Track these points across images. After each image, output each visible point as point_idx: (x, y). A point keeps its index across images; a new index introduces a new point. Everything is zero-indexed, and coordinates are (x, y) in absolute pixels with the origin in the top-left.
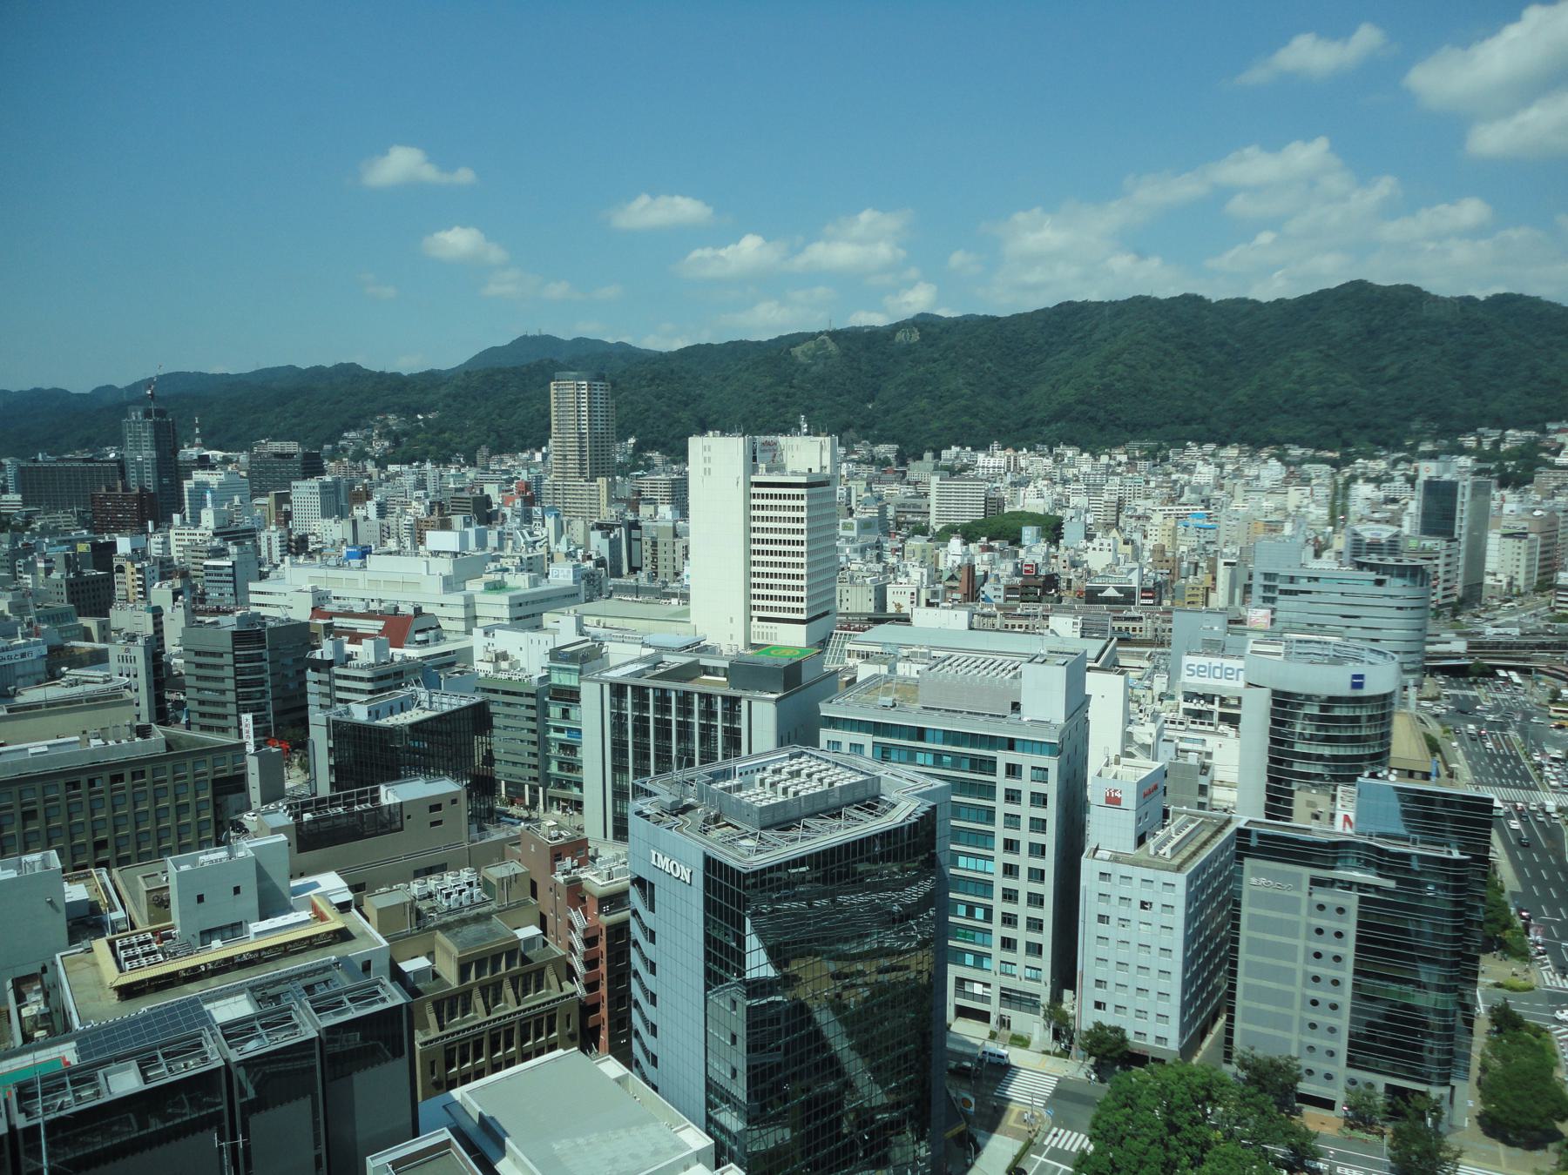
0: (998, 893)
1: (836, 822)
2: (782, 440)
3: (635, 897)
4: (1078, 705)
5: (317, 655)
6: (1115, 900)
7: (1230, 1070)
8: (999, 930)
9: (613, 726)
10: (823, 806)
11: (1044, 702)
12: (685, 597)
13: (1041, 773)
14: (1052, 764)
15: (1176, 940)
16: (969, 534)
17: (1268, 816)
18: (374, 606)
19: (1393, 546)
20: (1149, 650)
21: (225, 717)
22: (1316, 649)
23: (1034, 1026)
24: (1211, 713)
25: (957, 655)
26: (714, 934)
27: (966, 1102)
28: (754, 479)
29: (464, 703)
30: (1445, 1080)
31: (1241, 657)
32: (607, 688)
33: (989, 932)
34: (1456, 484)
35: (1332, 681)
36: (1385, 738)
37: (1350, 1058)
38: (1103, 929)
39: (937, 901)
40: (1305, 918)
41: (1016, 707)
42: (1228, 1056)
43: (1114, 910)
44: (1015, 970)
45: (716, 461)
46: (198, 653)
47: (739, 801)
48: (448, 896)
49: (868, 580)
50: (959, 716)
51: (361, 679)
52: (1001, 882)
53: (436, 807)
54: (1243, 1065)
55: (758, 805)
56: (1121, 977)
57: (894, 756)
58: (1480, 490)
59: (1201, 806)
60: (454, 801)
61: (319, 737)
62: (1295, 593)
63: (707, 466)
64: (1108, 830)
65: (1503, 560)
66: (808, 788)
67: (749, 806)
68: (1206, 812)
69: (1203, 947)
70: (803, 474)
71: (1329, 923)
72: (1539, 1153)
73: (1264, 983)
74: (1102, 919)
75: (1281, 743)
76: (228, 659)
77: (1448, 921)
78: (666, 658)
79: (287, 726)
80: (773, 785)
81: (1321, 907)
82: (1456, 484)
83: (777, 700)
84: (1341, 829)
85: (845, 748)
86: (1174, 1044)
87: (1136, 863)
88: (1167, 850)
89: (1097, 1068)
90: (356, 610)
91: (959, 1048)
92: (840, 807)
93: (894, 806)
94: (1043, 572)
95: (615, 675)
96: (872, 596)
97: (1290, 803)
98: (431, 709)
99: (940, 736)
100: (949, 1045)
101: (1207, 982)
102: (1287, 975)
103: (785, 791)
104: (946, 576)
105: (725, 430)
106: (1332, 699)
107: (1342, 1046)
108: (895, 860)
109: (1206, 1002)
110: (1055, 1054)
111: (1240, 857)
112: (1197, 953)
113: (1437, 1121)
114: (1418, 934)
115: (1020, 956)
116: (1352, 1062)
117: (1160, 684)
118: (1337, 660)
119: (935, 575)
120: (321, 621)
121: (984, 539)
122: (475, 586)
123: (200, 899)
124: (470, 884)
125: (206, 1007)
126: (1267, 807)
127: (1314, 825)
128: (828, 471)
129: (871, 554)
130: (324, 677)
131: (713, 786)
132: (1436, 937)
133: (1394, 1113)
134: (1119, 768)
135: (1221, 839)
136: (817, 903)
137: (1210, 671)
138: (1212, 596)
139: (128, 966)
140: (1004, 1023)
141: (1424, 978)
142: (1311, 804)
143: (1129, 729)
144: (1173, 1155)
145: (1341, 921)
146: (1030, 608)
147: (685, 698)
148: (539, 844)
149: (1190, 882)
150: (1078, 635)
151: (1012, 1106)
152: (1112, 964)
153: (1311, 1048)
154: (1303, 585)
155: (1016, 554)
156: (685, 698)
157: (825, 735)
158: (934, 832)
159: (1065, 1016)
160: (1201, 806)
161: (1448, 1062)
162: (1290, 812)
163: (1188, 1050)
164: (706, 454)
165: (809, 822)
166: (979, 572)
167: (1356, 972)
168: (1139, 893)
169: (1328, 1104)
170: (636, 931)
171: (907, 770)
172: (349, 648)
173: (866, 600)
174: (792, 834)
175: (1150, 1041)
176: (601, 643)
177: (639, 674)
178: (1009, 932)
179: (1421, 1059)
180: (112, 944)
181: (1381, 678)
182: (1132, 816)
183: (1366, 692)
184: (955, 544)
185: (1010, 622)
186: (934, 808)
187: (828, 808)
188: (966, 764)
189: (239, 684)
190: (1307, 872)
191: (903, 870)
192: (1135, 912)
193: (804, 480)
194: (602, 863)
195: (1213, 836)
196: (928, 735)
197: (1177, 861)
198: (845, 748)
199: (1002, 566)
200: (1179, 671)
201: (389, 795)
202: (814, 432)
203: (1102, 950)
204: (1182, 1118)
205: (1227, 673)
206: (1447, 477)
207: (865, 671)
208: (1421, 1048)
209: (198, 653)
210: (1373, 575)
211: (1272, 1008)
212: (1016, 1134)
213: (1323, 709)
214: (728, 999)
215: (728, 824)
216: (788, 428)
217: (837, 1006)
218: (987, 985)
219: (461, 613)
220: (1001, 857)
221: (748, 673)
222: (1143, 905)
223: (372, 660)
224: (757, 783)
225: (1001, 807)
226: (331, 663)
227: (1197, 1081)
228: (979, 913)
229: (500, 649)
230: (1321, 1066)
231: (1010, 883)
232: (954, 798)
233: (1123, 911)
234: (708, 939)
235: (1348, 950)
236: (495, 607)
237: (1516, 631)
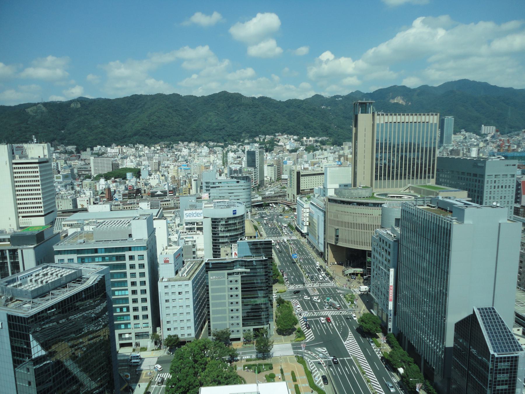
0: (130, 301)
1: (65, 289)
2: (25, 146)
4: (152, 232)
6: (170, 294)
7: (211, 338)
8: (132, 313)
10: (59, 285)
11: (140, 232)
13: (141, 257)
14: (145, 253)
15: (191, 302)
16: (107, 177)
17: (214, 257)
19: (240, 171)
20: (173, 211)
22: (222, 204)
23: (148, 343)
24: (194, 228)
25: (107, 220)
27: (127, 376)
28: (14, 161)
30: (267, 323)
31: (201, 209)
33: (129, 315)
35: (227, 213)
36: (243, 228)
37: (243, 324)
38: (167, 304)
39: (109, 309)
40: (227, 286)
41: (130, 236)
42: (210, 333)
43: (170, 297)
44: (139, 326)
47: (21, 290)
50: (110, 242)
52: (131, 297)
54: (214, 335)
55: (30, 290)
56: (175, 318)
57: (86, 260)
58: (261, 153)
59: (194, 258)
62: (215, 187)
64: (166, 271)
65: (269, 173)
66: (51, 279)
67: (26, 291)
68: (196, 260)
69: (199, 302)
70: (36, 159)
71: (233, 286)
72: (291, 336)
73: (218, 308)
74: (167, 301)
75: (215, 234)
77: (263, 278)
80: (36, 281)
81: (231, 281)
83: (34, 248)
84: (234, 257)
85: (66, 261)
86: (193, 335)
87: (176, 280)
88: (185, 274)
89: (170, 350)
91: (122, 358)
92: (66, 284)
93: (88, 279)
94: (135, 188)
96: (71, 203)
97: (219, 252)
99: (103, 250)
100: (119, 358)
101: (201, 313)
102: (223, 304)
103: (42, 282)
104: (100, 192)
106: (228, 219)
107: (240, 321)
108: (91, 298)
109: (201, 319)
110: (156, 350)
111: (207, 271)
112: (197, 304)
113: (266, 336)
114: (257, 283)
115: (141, 321)
116: (244, 325)
117: (178, 221)
118: (228, 207)
119: (96, 193)
121: (113, 178)
126: (213, 254)
127: (227, 257)
128: (47, 157)
129: (68, 187)
131: (9, 286)
132: (262, 283)
133: (256, 336)
134: (167, 250)
135: (201, 267)
136: (61, 322)
137: (193, 215)
138: (191, 190)
140: (137, 344)
141: (260, 295)
142: (225, 251)
143: (169, 237)
144: (196, 370)
146: (132, 201)
149: (193, 282)
150: (150, 208)
151: (143, 372)
152: (171, 315)
153: (232, 324)
154: (217, 185)
155: (125, 183)
157: (57, 258)
158: (105, 285)
159: (158, 336)
160: (194, 258)
161: (268, 317)
162: (220, 255)
163: (197, 336)
165: (53, 292)
166: (112, 190)
167: (242, 298)
168: (177, 290)
169: (239, 339)
171: (92, 265)
174: (47, 298)
175: (186, 336)
178: (136, 313)
179: (261, 319)
181: (241, 210)
182: (173, 265)
183: (237, 215)
184: (102, 181)
185: (125, 207)
186: (104, 276)
187: (61, 285)
188: (114, 258)
191: (94, 301)
192: (177, 296)
193: (37, 161)
195: (198, 267)
196: (99, 251)
197: (189, 277)
198: (66, 261)
199: (121, 187)
202: (39, 141)
203: (168, 311)
204: (198, 357)
205: (198, 215)
206: (252, 150)
207: (71, 231)
208: (261, 316)
210: (236, 180)
212: (145, 381)
213: (226, 222)
214: (25, 369)
216: (28, 140)
217: (74, 358)
218: (130, 334)
220: (130, 288)
221: (19, 239)
222: (179, 293)
224: (29, 281)
225: (128, 271)
227: (201, 344)
228: (125, 310)
230: (235, 329)
231: (135, 297)
232: (111, 271)
233: (173, 297)
234: (13, 348)
235: (239, 292)
237: (273, 193)
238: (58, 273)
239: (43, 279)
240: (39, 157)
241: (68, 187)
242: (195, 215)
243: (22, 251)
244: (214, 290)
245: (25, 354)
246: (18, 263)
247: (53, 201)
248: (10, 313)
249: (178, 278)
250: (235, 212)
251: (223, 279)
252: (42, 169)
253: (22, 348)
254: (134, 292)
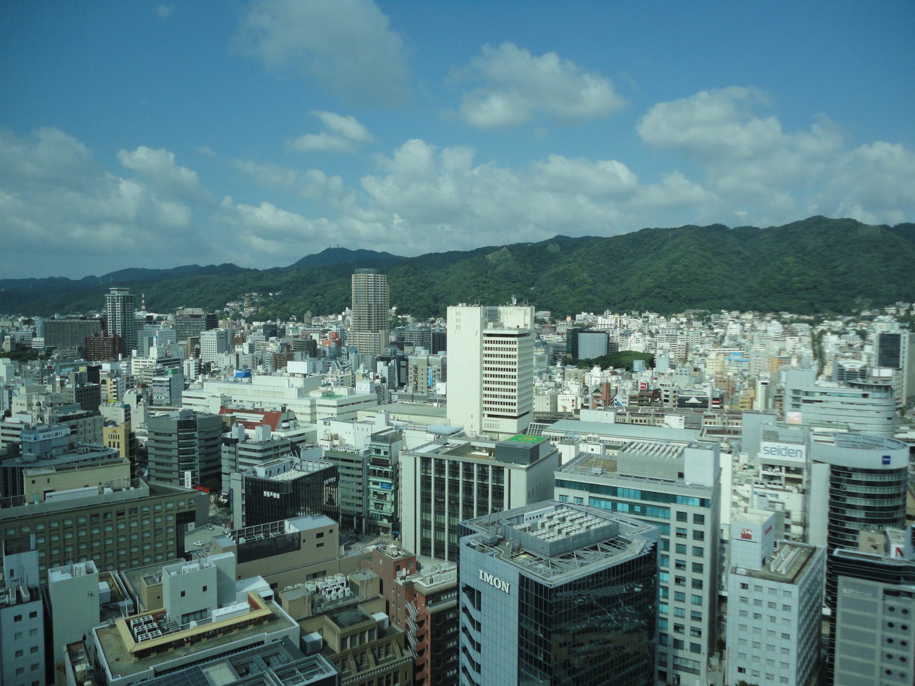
3: (465, 599)
4: (718, 472)
5: (228, 435)
9: (422, 482)
12: (443, 401)
13: (699, 519)
16: (603, 363)
18: (257, 406)
19: (863, 373)
20: (726, 436)
21: (171, 472)
24: (779, 478)
25: (636, 441)
26: (524, 625)
28: (486, 332)
29: (327, 466)
31: (798, 443)
32: (418, 460)
34: (899, 336)
35: (871, 459)
40: (880, 616)
41: (681, 475)
45: (463, 323)
46: (156, 434)
48: (330, 592)
49: (546, 392)
51: (255, 451)
53: (320, 535)
60: (331, 531)
61: (234, 484)
63: (458, 324)
64: (744, 556)
76: (175, 437)
78: (449, 441)
79: (211, 479)
81: (892, 609)
82: (899, 336)
83: (527, 469)
84: (893, 557)
85: (571, 499)
87: (764, 577)
90: (247, 408)
94: (652, 388)
95: (423, 451)
97: (855, 538)
98: (301, 470)
102: (870, 654)
103: (560, 532)
104: (591, 390)
105: (470, 302)
117: (744, 458)
119: (585, 389)
120: (228, 415)
121: (611, 368)
122: (316, 394)
123: (183, 594)
124: (342, 584)
125: (204, 671)
128: (529, 327)
129: (545, 376)
130: (232, 449)
137: (779, 451)
138: (755, 403)
139: (140, 638)
142: (871, 540)
145: (905, 618)
147: (468, 467)
148: (385, 559)
150: (683, 427)
154: (817, 397)
155: (631, 378)
156: (468, 467)
157: (558, 491)
160: (787, 537)
164: (458, 317)
166: (613, 388)
168: (766, 597)
170: (464, 619)
172: (247, 431)
173: (545, 404)
176: (401, 431)
177: (437, 452)
180: (128, 623)
182: (759, 546)
183: (892, 466)
184: (596, 370)
185: (635, 418)
186: (656, 544)
189: (181, 453)
190: (881, 586)
193: (516, 332)
194: (425, 572)
195: (808, 559)
197: (790, 577)
199: (625, 384)
200: (759, 451)
201: (290, 527)
202: (519, 303)
206: (893, 332)
209: (156, 434)
210: (860, 392)
211: (858, 675)
215: (526, 553)
216: (506, 302)
219: (308, 410)
221: (506, 452)
223: (261, 439)
224: (539, 526)
225: (674, 540)
226: (236, 441)
229: (334, 432)
234: (521, 629)
236: (327, 408)
238: (581, 520)
239: (561, 527)
241: (545, 376)
242: (784, 452)
243: (510, 471)
244: (849, 619)
245: (539, 648)
246: (502, 488)
247: (530, 396)
248: (523, 573)
249: (767, 573)
250: (886, 460)
251: (873, 600)
253: (536, 636)
254: (678, 580)
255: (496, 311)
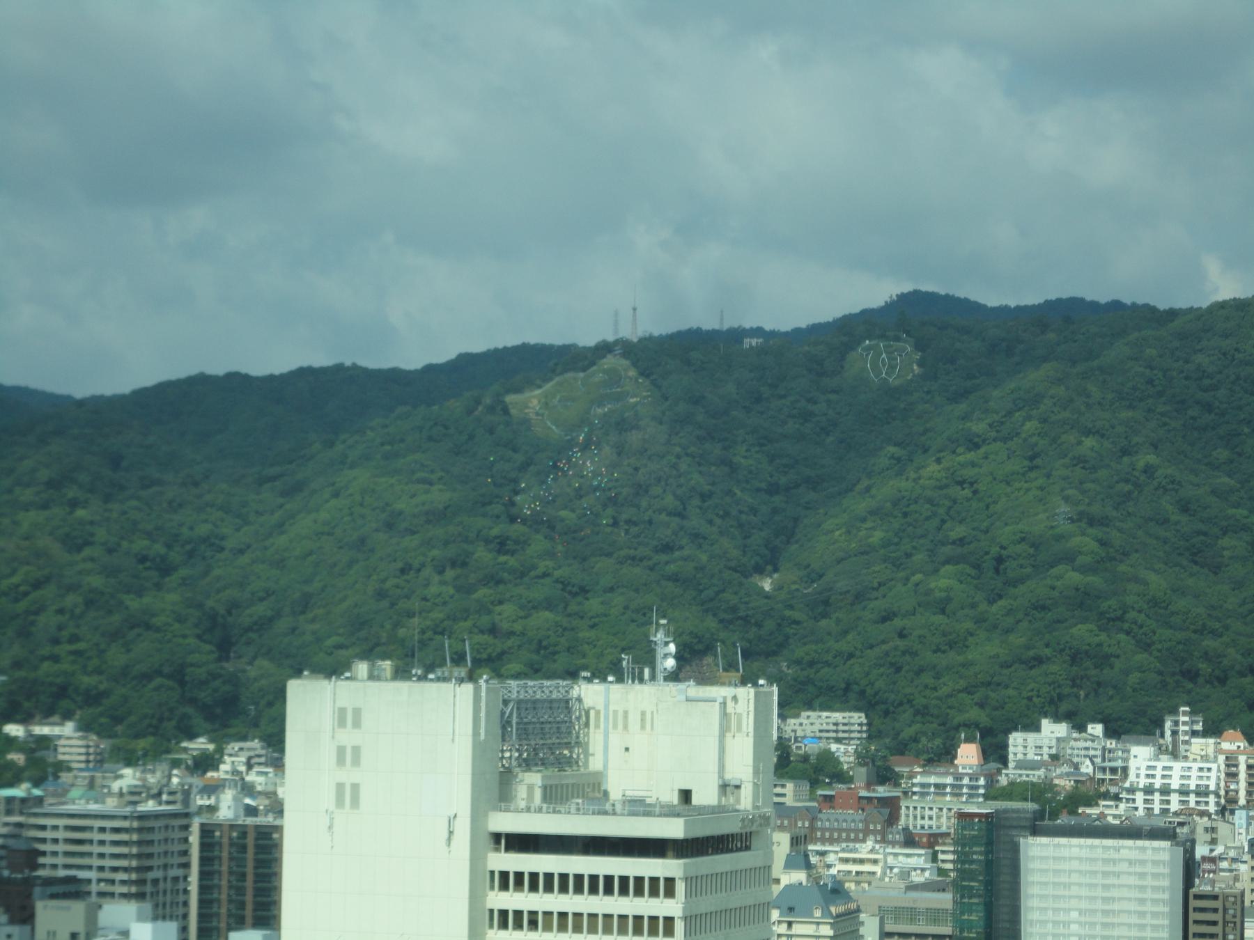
63: (348, 776)
70: (669, 812)
105: (415, 657)
128: (746, 800)
193: (674, 829)
202: (694, 661)
216: (623, 659)
240: (686, 795)
252: (708, 903)
255: (566, 704)
